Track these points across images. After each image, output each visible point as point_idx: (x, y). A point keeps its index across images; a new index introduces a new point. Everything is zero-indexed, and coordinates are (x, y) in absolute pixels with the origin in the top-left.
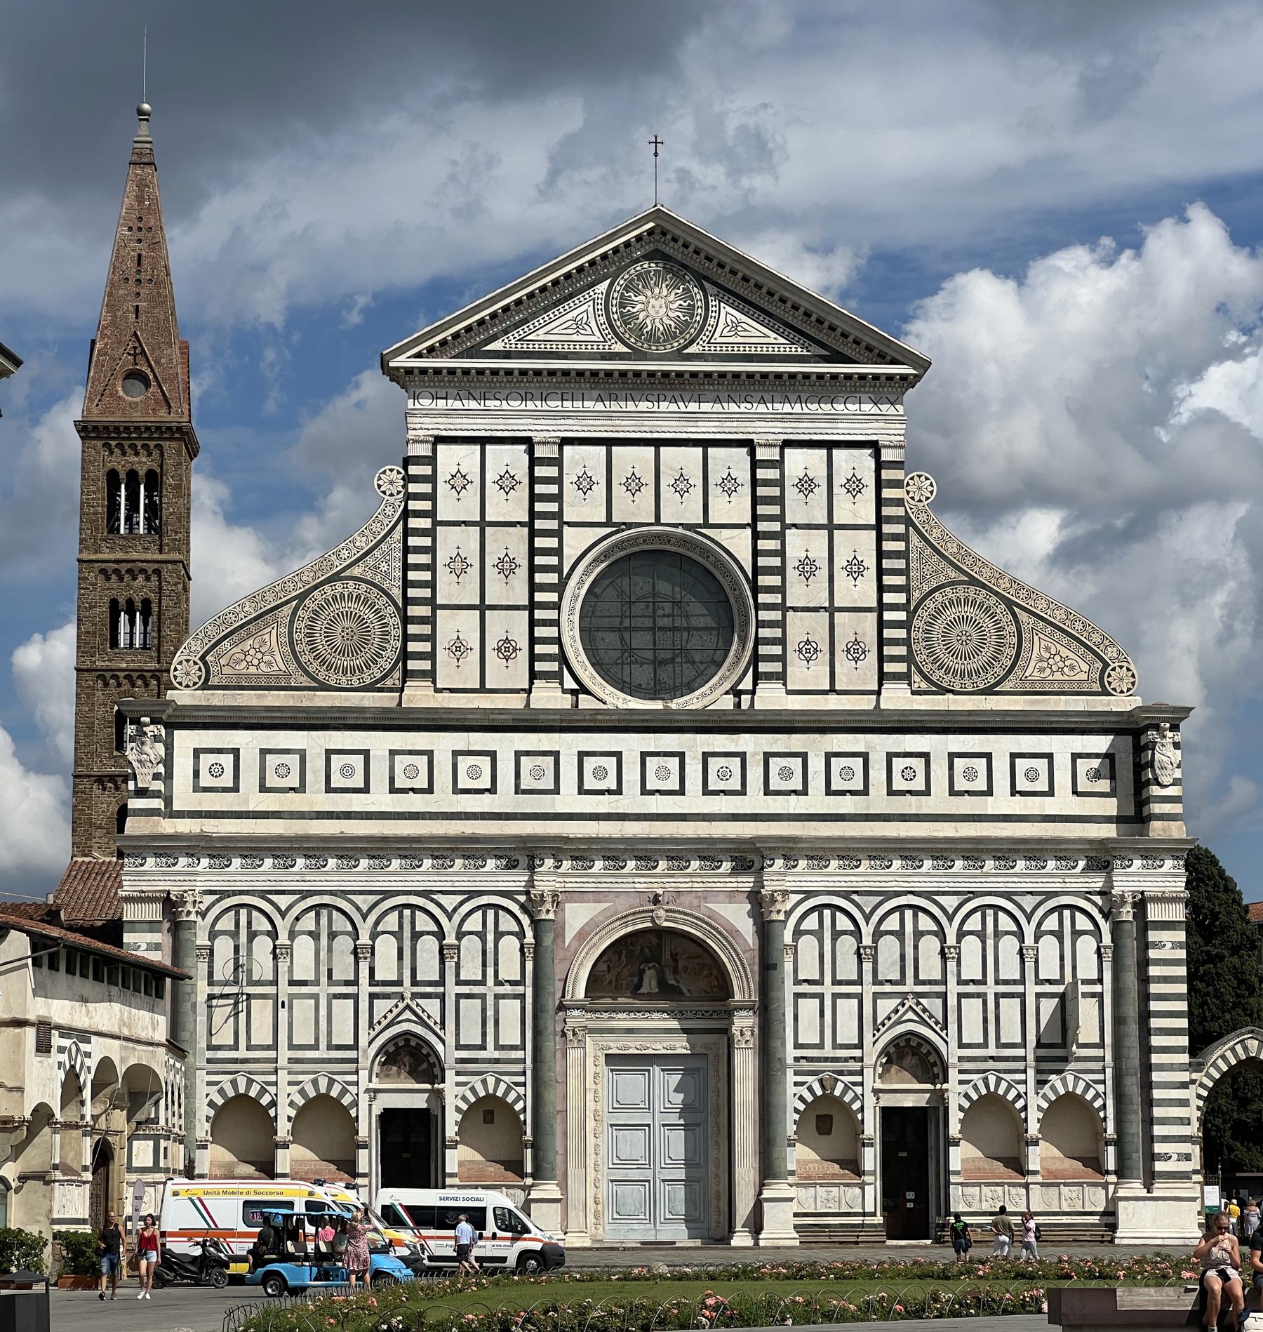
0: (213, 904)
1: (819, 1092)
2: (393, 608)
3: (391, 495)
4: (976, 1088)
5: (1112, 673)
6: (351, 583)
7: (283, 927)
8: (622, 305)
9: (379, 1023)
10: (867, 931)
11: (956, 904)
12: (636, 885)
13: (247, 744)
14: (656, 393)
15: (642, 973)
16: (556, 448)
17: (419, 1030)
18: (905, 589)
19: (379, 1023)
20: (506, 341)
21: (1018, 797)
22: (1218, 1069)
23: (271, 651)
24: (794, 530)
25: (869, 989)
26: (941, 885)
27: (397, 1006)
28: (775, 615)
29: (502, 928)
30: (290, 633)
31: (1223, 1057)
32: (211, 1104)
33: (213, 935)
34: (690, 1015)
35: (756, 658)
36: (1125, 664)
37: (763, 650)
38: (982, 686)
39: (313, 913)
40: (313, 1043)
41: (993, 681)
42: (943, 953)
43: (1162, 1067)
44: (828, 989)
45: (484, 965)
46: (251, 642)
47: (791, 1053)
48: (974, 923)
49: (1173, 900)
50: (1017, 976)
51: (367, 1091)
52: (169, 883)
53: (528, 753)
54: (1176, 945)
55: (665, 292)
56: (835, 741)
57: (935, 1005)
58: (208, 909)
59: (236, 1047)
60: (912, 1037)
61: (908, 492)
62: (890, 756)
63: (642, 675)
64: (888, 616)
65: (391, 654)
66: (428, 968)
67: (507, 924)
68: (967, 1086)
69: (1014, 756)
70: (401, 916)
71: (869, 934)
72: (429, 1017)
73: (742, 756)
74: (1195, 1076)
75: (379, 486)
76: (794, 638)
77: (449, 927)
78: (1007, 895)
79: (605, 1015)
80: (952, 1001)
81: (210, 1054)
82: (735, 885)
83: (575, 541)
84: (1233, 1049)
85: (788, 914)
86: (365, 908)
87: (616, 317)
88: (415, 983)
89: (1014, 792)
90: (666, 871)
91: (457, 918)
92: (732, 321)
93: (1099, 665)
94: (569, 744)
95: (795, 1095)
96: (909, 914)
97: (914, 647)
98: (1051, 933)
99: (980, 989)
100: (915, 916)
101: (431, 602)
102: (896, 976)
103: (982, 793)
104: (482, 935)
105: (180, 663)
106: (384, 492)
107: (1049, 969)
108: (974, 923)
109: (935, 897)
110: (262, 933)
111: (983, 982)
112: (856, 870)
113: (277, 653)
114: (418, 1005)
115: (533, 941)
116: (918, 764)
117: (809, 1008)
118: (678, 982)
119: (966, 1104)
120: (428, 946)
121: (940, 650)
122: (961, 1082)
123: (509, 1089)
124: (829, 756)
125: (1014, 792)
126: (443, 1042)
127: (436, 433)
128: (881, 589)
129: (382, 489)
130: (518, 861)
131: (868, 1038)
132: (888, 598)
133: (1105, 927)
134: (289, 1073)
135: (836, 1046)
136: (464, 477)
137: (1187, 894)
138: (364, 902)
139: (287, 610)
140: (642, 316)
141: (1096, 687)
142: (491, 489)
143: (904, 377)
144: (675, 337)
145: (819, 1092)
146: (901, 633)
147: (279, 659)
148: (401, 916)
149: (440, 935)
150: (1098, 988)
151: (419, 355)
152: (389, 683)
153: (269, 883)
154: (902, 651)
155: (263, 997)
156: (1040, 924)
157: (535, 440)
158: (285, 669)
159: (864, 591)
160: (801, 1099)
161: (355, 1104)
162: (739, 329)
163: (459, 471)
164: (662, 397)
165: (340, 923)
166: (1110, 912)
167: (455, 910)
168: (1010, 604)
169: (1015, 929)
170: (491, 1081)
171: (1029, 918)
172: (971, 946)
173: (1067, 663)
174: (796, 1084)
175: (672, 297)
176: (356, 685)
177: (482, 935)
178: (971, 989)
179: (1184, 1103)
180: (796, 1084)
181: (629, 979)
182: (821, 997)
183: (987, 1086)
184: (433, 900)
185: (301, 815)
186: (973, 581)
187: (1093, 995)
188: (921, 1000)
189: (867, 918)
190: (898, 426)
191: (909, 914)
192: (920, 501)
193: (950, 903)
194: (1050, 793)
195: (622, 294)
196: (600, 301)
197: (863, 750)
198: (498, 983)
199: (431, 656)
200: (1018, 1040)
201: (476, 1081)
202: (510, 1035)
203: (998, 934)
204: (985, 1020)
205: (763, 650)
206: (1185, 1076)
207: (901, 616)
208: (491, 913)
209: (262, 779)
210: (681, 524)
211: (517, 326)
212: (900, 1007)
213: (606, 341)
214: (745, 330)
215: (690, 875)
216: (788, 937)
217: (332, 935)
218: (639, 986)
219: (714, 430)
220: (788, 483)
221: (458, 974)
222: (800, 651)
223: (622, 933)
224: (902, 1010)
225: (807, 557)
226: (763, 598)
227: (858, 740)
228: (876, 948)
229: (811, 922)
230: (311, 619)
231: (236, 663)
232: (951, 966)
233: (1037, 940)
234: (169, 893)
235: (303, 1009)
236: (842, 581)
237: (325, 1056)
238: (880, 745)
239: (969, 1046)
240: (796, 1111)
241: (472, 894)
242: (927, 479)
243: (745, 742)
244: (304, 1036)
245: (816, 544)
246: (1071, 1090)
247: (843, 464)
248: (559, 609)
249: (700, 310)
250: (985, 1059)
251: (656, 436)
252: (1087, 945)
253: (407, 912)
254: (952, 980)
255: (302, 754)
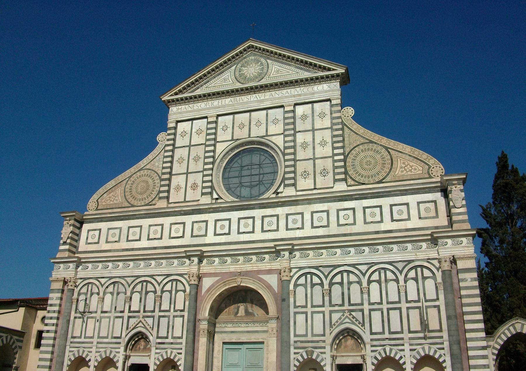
0: (81, 283)
1: (306, 357)
2: (158, 177)
3: (162, 141)
4: (380, 354)
5: (433, 169)
6: (146, 171)
7: (102, 290)
8: (240, 71)
9: (130, 328)
10: (326, 283)
11: (366, 269)
12: (230, 269)
13: (104, 227)
14: (250, 96)
15: (239, 307)
16: (215, 118)
17: (144, 330)
18: (343, 147)
19: (130, 328)
20: (202, 88)
21: (395, 223)
22: (502, 339)
23: (118, 195)
24: (299, 133)
25: (327, 309)
26: (359, 260)
27: (137, 321)
28: (292, 163)
29: (178, 288)
30: (125, 189)
31: (504, 333)
32: (70, 360)
33: (79, 294)
34: (257, 324)
35: (284, 179)
36: (438, 165)
37: (287, 176)
38: (377, 181)
39: (113, 285)
40: (106, 336)
41: (381, 178)
42: (362, 292)
43: (472, 340)
44: (309, 310)
45: (170, 304)
46: (112, 193)
47: (292, 338)
48: (375, 276)
49: (469, 258)
50: (397, 300)
51: (123, 355)
52: (66, 275)
53: (196, 222)
54: (473, 280)
55: (254, 65)
56: (315, 207)
57: (359, 315)
58: (79, 285)
59: (80, 337)
60: (350, 331)
61: (343, 114)
62: (338, 211)
63: (245, 192)
64: (336, 158)
65: (155, 193)
66: (150, 306)
67: (180, 287)
68: (375, 353)
69: (391, 206)
70: (142, 285)
71: (327, 284)
72: (148, 325)
73: (277, 216)
74: (491, 343)
75: (158, 139)
76: (300, 169)
77: (159, 289)
78: (390, 263)
79: (223, 325)
80: (366, 312)
81: (72, 340)
82: (270, 267)
83: (220, 148)
84: (508, 329)
85: (292, 277)
86: (130, 282)
87: (237, 75)
88: (145, 311)
89: (393, 220)
90: (243, 263)
91: (162, 285)
92: (277, 70)
93: (427, 167)
94: (211, 217)
95: (294, 358)
96: (345, 275)
97: (348, 169)
98: (412, 279)
99: (380, 306)
100: (348, 275)
101: (170, 173)
102: (340, 302)
103: (378, 222)
104: (170, 292)
105: (90, 203)
106: (160, 141)
107: (412, 295)
108: (375, 276)
109: (356, 266)
110: (95, 293)
111: (381, 303)
112: (321, 257)
113: (120, 196)
114: (145, 320)
115: (189, 293)
116: (350, 213)
117: (301, 318)
118: (253, 311)
119: (376, 362)
120: (151, 296)
121: (359, 169)
122: (372, 351)
123: (175, 356)
124: (312, 213)
125: (393, 220)
126: (152, 336)
127: (177, 119)
128: (334, 148)
129: (159, 140)
130: (185, 262)
131: (328, 331)
132: (336, 151)
133: (439, 275)
134: (97, 348)
135: (313, 335)
136: (185, 132)
137: (475, 255)
138: (129, 280)
139: (125, 182)
140: (246, 74)
141: (427, 176)
142: (194, 134)
143: (338, 75)
144: (257, 78)
145: (306, 357)
146: (342, 164)
147: (120, 198)
148: (142, 285)
149: (155, 292)
150: (437, 303)
151: (172, 95)
152: (154, 202)
153: (99, 274)
154: (343, 170)
155: (92, 317)
156: (406, 275)
157: (208, 116)
158: (121, 201)
159: (328, 150)
160: (298, 360)
161: (118, 361)
162: (279, 71)
163: (184, 131)
164: (252, 97)
165: (121, 289)
166: (440, 268)
167: (161, 282)
168: (387, 149)
169: (395, 278)
170: (169, 352)
171: (401, 272)
172: (374, 287)
173: (413, 168)
174: (295, 353)
175: (257, 66)
176: (143, 204)
177: (170, 292)
178: (376, 306)
179: (485, 357)
180: (295, 353)
181: (233, 310)
182: (306, 313)
183: (385, 353)
184: (154, 279)
185: (118, 250)
186: (371, 142)
187: (435, 306)
188: (353, 313)
189: (326, 277)
190: (338, 92)
191: (345, 275)
192: (348, 117)
193: (363, 268)
194: (409, 219)
195: (240, 68)
196: (232, 72)
197: (327, 209)
198: (175, 311)
199: (168, 191)
200: (399, 330)
201: (163, 352)
202: (178, 332)
203: (386, 281)
204: (383, 321)
205: (287, 176)
206: (484, 343)
207: (342, 157)
208: (174, 283)
209: (107, 238)
210: (258, 137)
211: (205, 84)
212: (342, 317)
213: (234, 83)
214: (281, 72)
215: (251, 264)
216: (291, 287)
217: (118, 294)
218: (237, 313)
219: (269, 104)
220: (297, 118)
221: (160, 308)
222: (302, 175)
223: (224, 289)
224: (343, 318)
225: (304, 142)
226: (287, 157)
227: (324, 206)
228: (330, 291)
229: (302, 281)
230: (132, 184)
231: (107, 201)
232: (365, 296)
233: (405, 282)
234: (65, 279)
235: (105, 322)
236: (318, 149)
237: (110, 341)
238: (334, 206)
239: (376, 334)
240: (295, 366)
241: (168, 275)
242: (350, 109)
243: (279, 211)
244: (103, 333)
245: (308, 137)
246: (427, 353)
247: (318, 109)
248: (212, 170)
249: (266, 69)
250: (384, 340)
251: (249, 109)
252: (430, 284)
253: (145, 284)
254: (366, 303)
255: (120, 229)
